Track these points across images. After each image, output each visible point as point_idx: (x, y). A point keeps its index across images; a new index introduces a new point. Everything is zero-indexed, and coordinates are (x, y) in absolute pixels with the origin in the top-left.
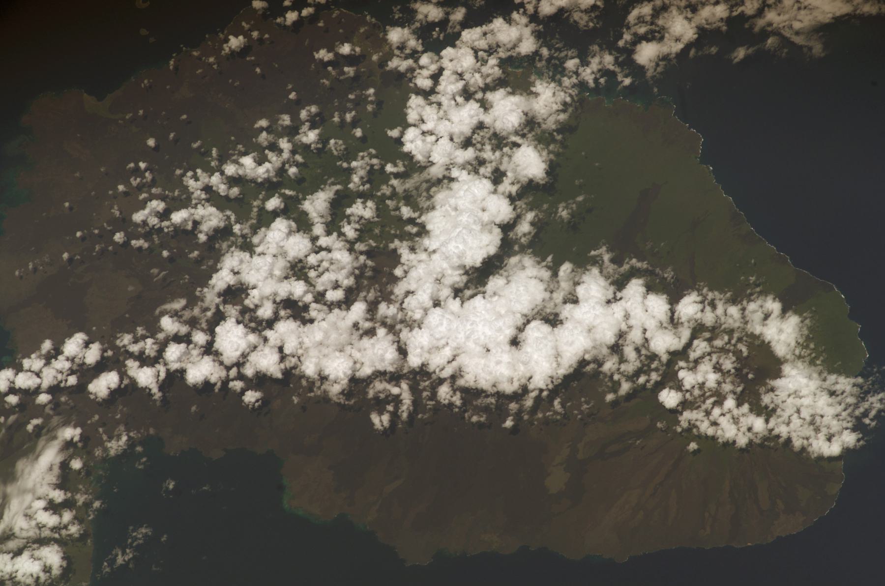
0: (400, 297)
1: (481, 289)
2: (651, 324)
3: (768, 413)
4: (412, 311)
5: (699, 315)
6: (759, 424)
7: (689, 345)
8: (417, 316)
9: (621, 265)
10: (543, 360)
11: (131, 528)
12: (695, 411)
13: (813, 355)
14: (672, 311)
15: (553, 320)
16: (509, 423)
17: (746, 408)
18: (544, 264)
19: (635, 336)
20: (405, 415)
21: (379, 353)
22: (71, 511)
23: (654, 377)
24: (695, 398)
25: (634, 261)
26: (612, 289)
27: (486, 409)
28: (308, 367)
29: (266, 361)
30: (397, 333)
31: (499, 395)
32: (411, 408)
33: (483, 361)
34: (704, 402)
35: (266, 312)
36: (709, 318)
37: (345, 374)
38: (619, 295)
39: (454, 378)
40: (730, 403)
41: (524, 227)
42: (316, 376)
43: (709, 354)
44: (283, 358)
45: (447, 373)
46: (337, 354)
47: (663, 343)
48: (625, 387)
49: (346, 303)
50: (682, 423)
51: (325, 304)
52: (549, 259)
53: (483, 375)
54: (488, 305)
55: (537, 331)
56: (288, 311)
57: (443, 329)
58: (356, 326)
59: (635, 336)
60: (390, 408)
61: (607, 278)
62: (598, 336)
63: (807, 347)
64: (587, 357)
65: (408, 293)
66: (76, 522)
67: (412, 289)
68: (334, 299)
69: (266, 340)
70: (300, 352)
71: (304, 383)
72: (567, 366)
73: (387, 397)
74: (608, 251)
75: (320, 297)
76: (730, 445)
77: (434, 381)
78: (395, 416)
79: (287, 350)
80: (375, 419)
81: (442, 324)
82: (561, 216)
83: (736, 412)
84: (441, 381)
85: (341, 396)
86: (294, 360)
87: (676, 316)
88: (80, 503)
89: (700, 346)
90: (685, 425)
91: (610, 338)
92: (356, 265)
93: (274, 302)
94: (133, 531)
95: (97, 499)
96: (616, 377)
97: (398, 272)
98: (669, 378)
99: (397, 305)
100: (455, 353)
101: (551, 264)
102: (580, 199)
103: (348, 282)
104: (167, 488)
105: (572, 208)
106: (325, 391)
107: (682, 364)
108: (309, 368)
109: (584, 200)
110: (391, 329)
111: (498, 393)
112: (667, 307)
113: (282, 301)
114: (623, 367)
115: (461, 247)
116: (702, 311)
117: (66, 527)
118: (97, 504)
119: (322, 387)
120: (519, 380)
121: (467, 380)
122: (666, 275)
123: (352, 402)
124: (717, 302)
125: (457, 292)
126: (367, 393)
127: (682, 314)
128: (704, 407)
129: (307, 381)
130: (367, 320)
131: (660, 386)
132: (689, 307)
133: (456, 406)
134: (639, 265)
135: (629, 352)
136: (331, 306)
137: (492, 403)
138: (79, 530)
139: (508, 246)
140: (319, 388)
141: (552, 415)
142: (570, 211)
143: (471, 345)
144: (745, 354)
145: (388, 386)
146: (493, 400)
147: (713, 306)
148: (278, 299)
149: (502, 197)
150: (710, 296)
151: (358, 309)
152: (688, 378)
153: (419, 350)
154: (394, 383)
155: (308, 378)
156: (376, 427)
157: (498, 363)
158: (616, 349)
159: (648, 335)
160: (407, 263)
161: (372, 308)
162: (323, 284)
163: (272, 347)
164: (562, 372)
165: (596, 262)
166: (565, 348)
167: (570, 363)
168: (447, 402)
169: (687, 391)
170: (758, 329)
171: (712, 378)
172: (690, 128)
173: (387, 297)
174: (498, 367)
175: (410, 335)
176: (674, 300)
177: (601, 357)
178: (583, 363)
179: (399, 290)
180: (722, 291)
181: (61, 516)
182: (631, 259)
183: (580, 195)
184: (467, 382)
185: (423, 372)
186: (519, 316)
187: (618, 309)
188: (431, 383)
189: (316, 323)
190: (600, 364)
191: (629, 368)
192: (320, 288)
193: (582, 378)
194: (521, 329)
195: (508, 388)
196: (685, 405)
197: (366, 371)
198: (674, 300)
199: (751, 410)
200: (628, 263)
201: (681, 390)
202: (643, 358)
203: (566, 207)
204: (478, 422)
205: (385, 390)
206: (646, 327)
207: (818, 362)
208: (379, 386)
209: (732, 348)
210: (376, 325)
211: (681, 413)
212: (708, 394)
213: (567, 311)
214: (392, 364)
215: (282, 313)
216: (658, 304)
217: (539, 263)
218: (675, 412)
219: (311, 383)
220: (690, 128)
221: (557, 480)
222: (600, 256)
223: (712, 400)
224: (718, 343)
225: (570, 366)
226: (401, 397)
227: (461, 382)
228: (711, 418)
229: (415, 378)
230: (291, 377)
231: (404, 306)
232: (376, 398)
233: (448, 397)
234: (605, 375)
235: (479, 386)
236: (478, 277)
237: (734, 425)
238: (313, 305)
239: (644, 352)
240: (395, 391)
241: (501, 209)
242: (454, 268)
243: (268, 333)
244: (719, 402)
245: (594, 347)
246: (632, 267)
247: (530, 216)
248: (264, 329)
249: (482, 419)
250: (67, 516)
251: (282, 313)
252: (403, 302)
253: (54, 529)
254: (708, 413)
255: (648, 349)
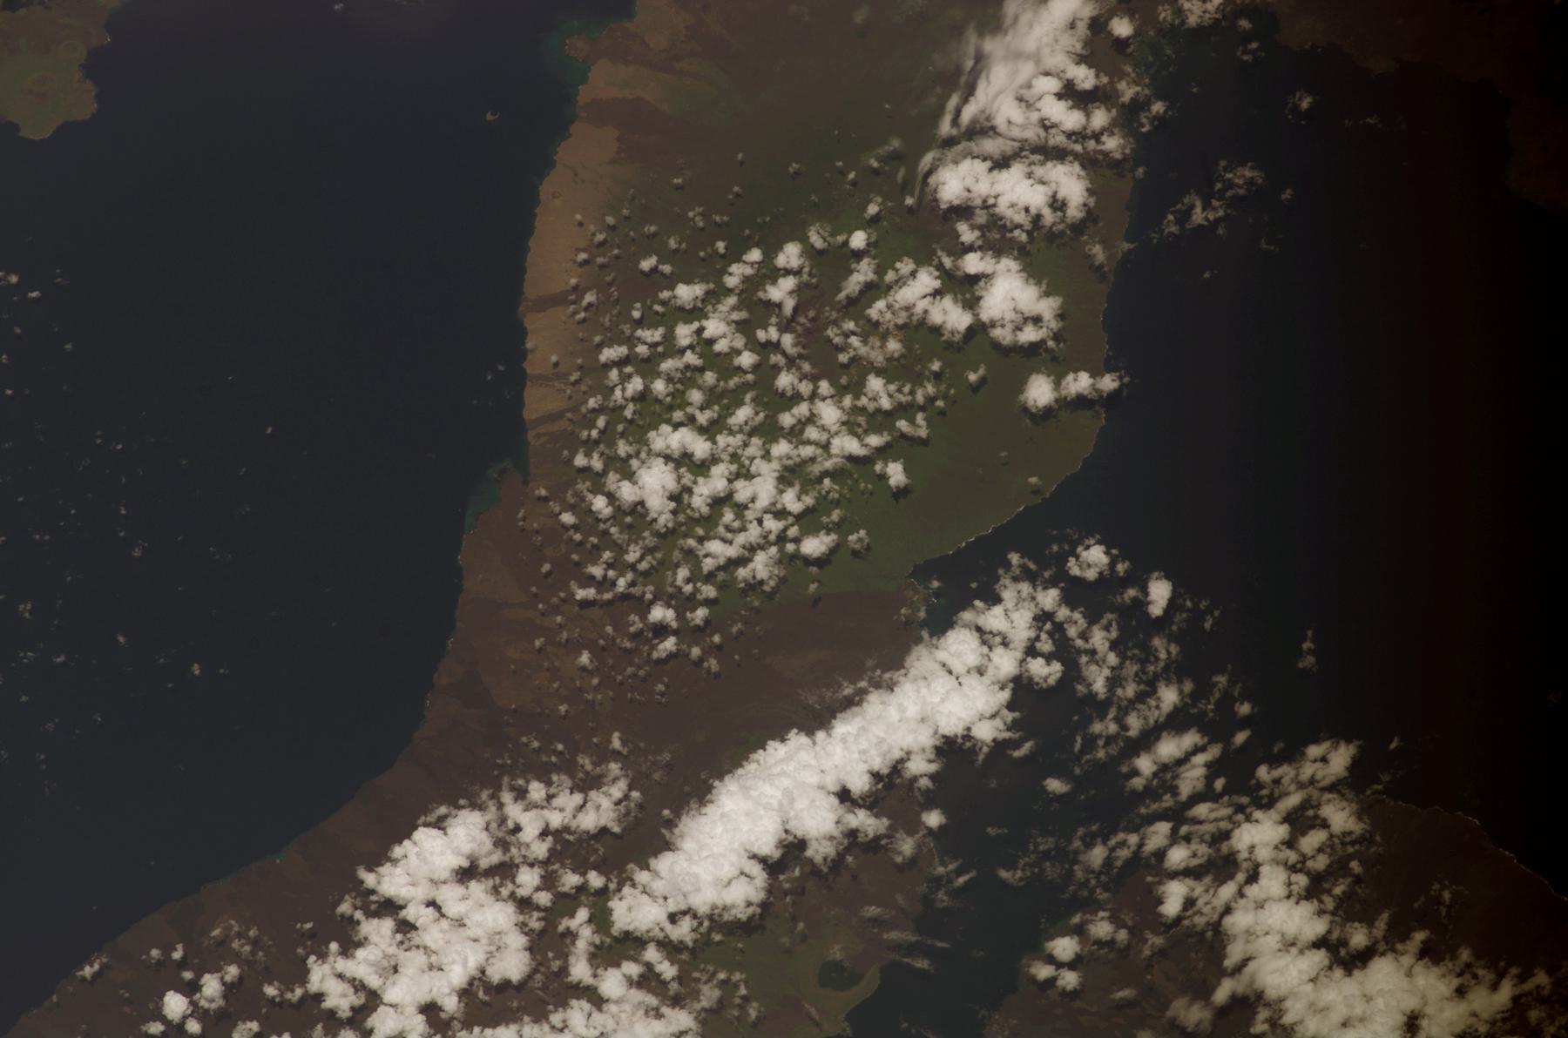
11: (1223, 163)
22: (1109, 110)
66: (1116, 131)
88: (1126, 99)
94: (1226, 170)
95: (1159, 97)
104: (1296, 107)
117: (1097, 136)
118: (1158, 107)
138: (1123, 147)
181: (1088, 115)
250: (1100, 118)
253: (1070, 135)
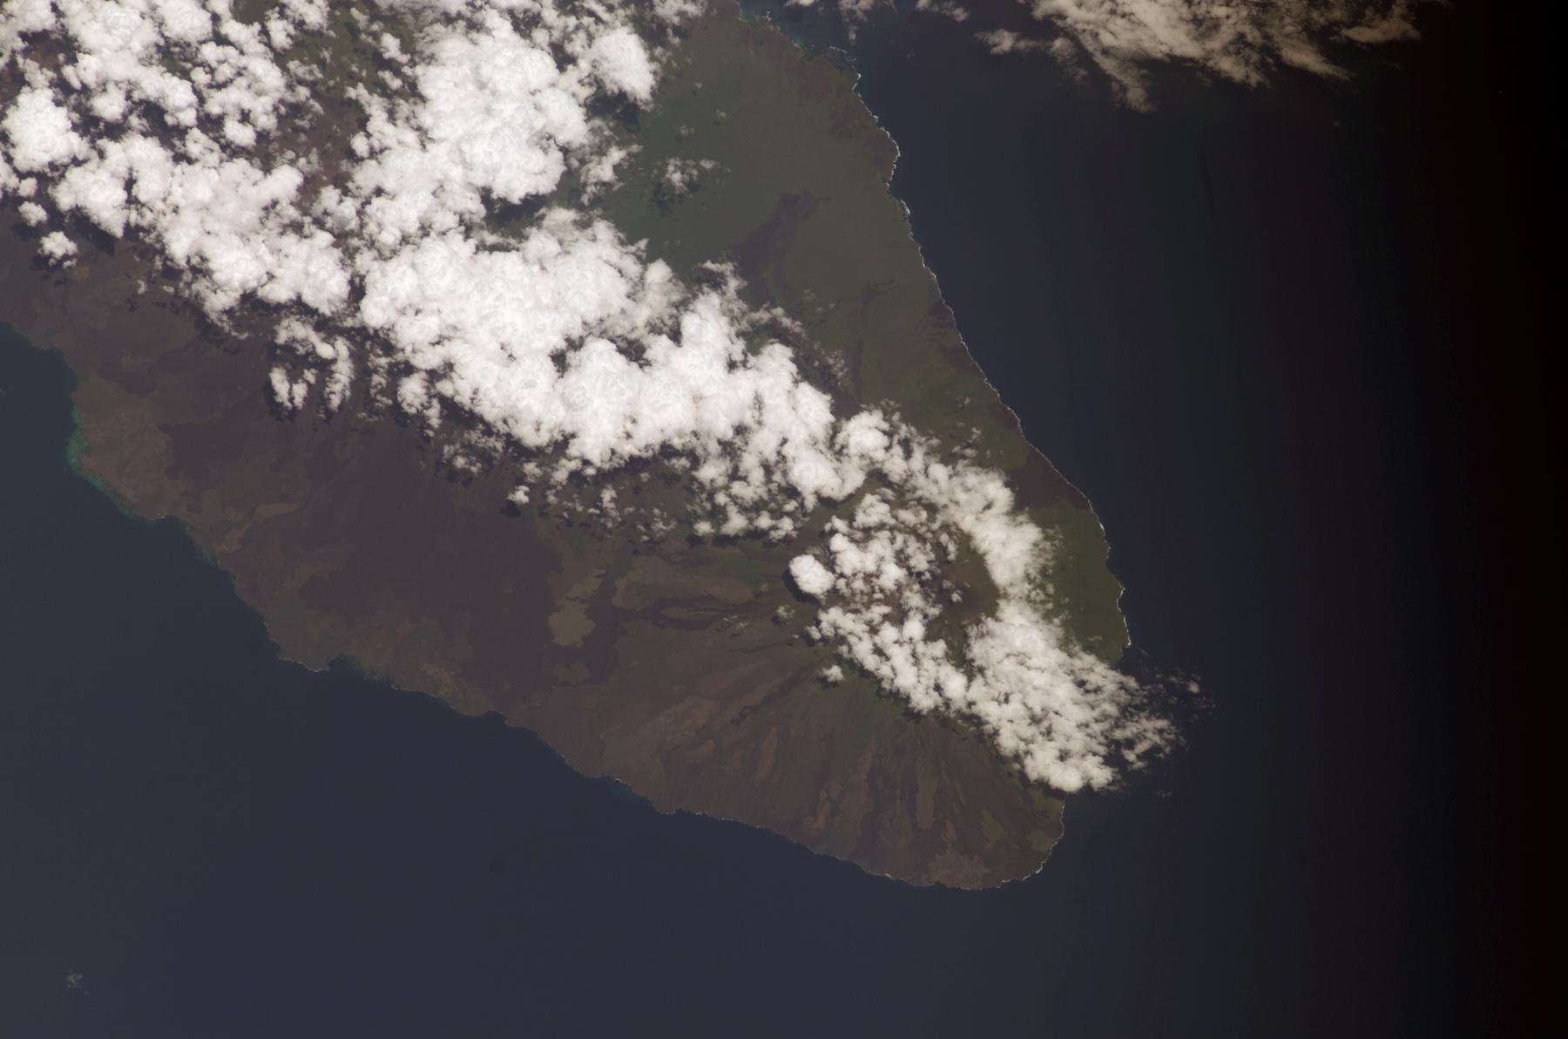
0: (366, 191)
1: (512, 241)
2: (798, 435)
3: (970, 670)
4: (380, 226)
5: (879, 455)
6: (955, 684)
7: (854, 498)
8: (389, 237)
9: (755, 309)
10: (605, 412)
12: (850, 616)
13: (1050, 606)
14: (835, 430)
15: (634, 351)
16: (521, 495)
17: (939, 647)
18: (633, 249)
19: (763, 443)
20: (335, 401)
21: (311, 272)
23: (787, 525)
24: (853, 594)
25: (779, 311)
26: (740, 345)
27: (484, 456)
28: (178, 240)
29: (96, 193)
30: (350, 254)
31: (512, 442)
32: (348, 393)
33: (496, 369)
34: (868, 606)
35: (110, 106)
36: (896, 466)
37: (242, 285)
38: (752, 360)
39: (433, 376)
40: (914, 627)
41: (603, 170)
42: (183, 263)
43: (892, 529)
44: (132, 201)
45: (429, 359)
46: (236, 240)
47: (814, 475)
48: (736, 523)
49: (263, 154)
50: (824, 625)
51: (216, 140)
52: (643, 244)
53: (494, 394)
54: (526, 280)
55: (601, 357)
56: (144, 121)
57: (444, 283)
58: (271, 207)
59: (763, 443)
60: (310, 376)
61: (733, 319)
62: (707, 416)
63: (1042, 587)
64: (677, 443)
65: (379, 192)
67: (389, 185)
68: (237, 141)
69: (102, 155)
70: (159, 205)
71: (158, 263)
72: (642, 444)
73: (308, 354)
74: (735, 273)
75: (211, 124)
76: (900, 699)
77: (397, 364)
78: (317, 394)
79: (143, 191)
80: (278, 379)
81: (443, 275)
82: (669, 180)
83: (921, 648)
84: (409, 369)
85: (225, 318)
86: (149, 217)
87: (840, 438)
89: (874, 510)
90: (828, 631)
91: (724, 428)
92: (290, 98)
93: (128, 97)
96: (721, 499)
97: (360, 144)
98: (813, 538)
99: (358, 204)
100: (445, 333)
101: (644, 255)
102: (707, 165)
103: (267, 122)
105: (690, 175)
106: (198, 294)
107: (839, 524)
108: (180, 246)
109: (711, 171)
110: (342, 238)
111: (509, 435)
112: (828, 418)
113: (142, 101)
114: (737, 488)
115: (496, 158)
116: (887, 449)
119: (195, 287)
120: (551, 431)
121: (459, 388)
122: (831, 361)
123: (245, 336)
124: (915, 446)
125: (468, 229)
126: (275, 333)
127: (852, 441)
128: (868, 615)
129: (164, 265)
130: (292, 203)
131: (793, 546)
132: (865, 432)
133: (430, 427)
134: (787, 322)
135: (750, 462)
136: (232, 151)
137: (495, 449)
139: (569, 190)
140: (189, 285)
141: (599, 516)
142: (687, 178)
143: (483, 335)
144: (952, 557)
145: (314, 338)
146: (499, 445)
147: (907, 447)
148: (136, 95)
149: (573, 100)
150: (904, 430)
151: (286, 180)
152: (851, 557)
153: (385, 299)
154: (322, 335)
155: (168, 259)
156: (279, 400)
157: (530, 385)
158: (729, 450)
159: (787, 450)
160: (376, 135)
161: (309, 190)
162: (222, 106)
163: (113, 175)
164: (629, 449)
165: (716, 282)
166: (646, 411)
167: (651, 441)
168: (413, 411)
169: (842, 575)
170: (967, 523)
171: (892, 574)
172: (879, 125)
173: (342, 183)
174: (526, 392)
175: (376, 265)
176: (844, 409)
177: (699, 452)
178: (667, 450)
179: (365, 176)
180: (922, 431)
182: (775, 306)
183: (710, 158)
184: (457, 392)
185: (382, 341)
186: (579, 321)
187: (745, 382)
188: (390, 364)
189: (197, 167)
190: (696, 461)
191: (748, 491)
192: (214, 108)
193: (659, 474)
194: (575, 344)
195: (531, 438)
196: (835, 597)
197: (279, 293)
198: (844, 409)
199: (948, 657)
200: (767, 310)
201: (834, 572)
202: (774, 486)
203: (683, 170)
204: (465, 471)
205: (304, 341)
206: (788, 436)
207: (1056, 621)
208: (293, 330)
209: (929, 535)
210: (307, 220)
211: (825, 609)
212: (878, 596)
213: (659, 347)
214: (330, 302)
215: (134, 121)
216: (815, 406)
217: (622, 243)
218: (810, 604)
219: (172, 272)
220: (879, 125)
221: (570, 625)
222: (722, 275)
223: (886, 609)
224: (907, 516)
225: (647, 447)
226: (334, 368)
227: (445, 387)
228: (877, 639)
229: (362, 344)
230: (140, 245)
231: (368, 209)
232: (289, 348)
233: (417, 403)
234: (702, 486)
235: (477, 410)
236: (506, 220)
237: (912, 667)
238: (196, 133)
239: (777, 477)
240: (325, 351)
241: (573, 125)
242: (470, 185)
243: (104, 143)
244: (898, 617)
245: (695, 434)
246: (774, 322)
247: (616, 155)
248: (101, 137)
249: (474, 469)
251: (134, 121)
252: (368, 202)
254: (873, 630)
255: (785, 473)
